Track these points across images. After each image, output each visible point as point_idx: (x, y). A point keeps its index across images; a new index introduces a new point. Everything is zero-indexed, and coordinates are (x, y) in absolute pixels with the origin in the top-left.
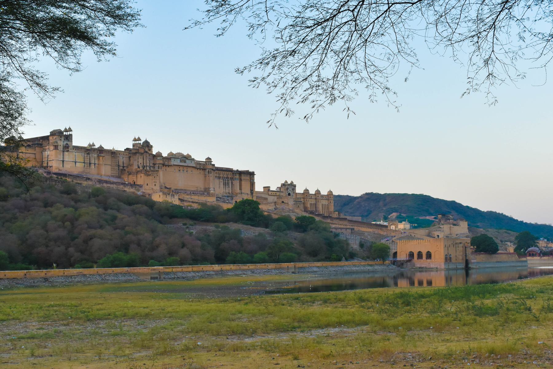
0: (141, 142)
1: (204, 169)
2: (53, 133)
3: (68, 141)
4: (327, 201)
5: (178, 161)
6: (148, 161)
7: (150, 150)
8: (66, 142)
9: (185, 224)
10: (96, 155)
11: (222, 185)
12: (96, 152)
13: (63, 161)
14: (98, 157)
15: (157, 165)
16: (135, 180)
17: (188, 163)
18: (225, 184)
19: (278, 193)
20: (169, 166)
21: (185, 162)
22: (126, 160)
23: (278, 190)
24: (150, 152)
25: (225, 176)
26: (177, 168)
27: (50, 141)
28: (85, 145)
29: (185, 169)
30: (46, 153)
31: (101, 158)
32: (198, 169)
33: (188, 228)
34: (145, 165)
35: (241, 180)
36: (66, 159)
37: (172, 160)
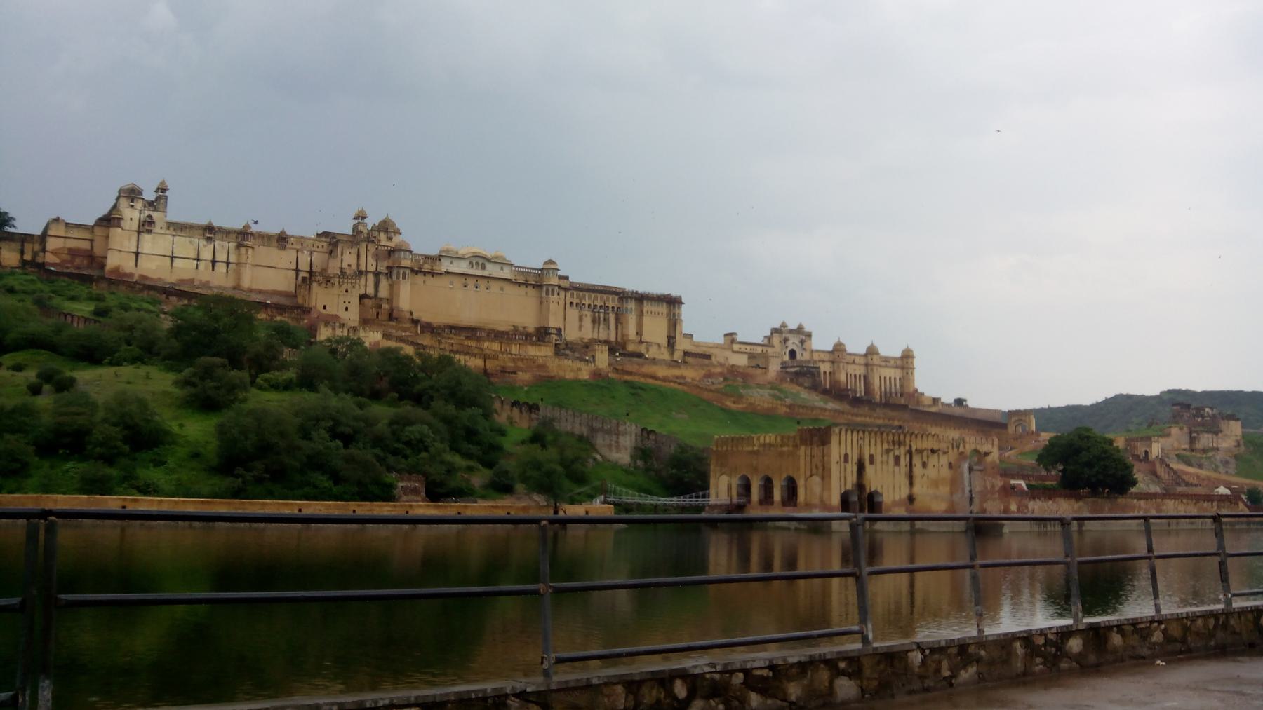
0: (372, 221)
1: (538, 286)
3: (156, 210)
6: (371, 261)
7: (390, 239)
10: (233, 245)
11: (587, 322)
13: (137, 254)
14: (239, 246)
15: (395, 271)
17: (492, 270)
18: (595, 321)
20: (433, 274)
21: (483, 267)
22: (318, 259)
25: (599, 303)
26: (458, 282)
29: (483, 284)
31: (243, 250)
32: (520, 284)
35: (641, 315)
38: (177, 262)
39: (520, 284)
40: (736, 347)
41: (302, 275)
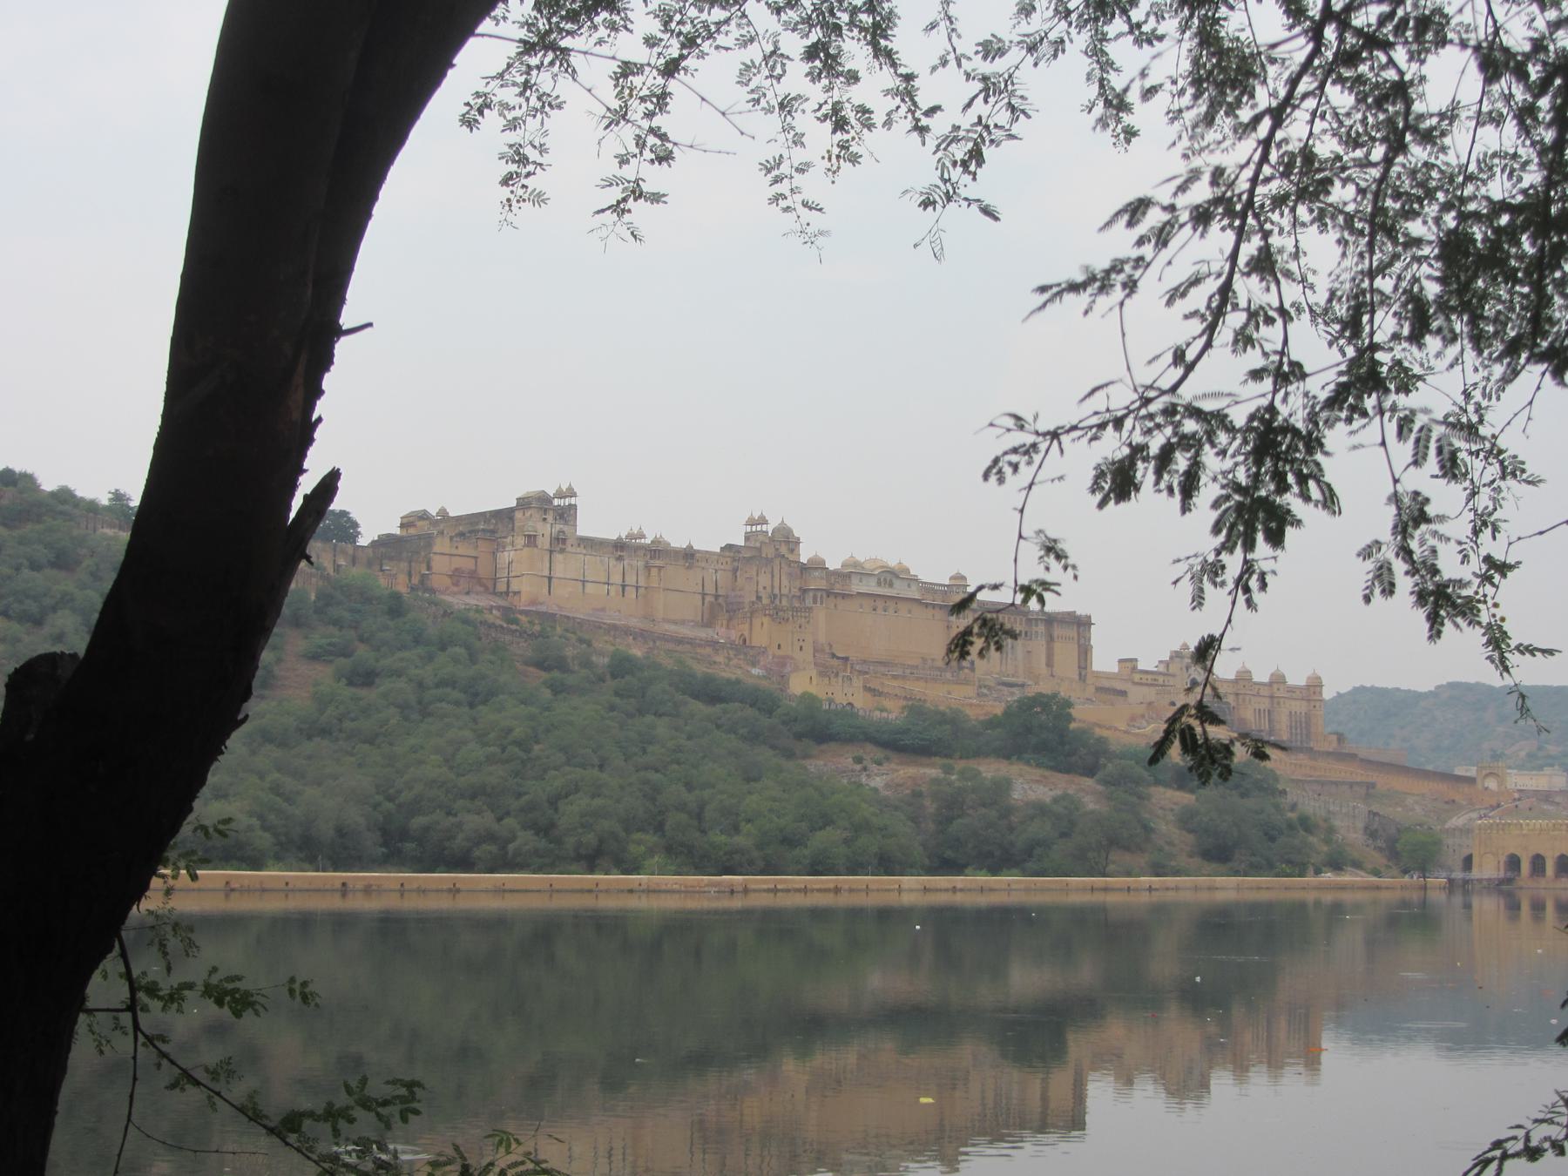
0: (769, 528)
2: (524, 503)
3: (566, 523)
4: (1304, 703)
5: (873, 582)
6: (785, 582)
7: (792, 551)
8: (558, 527)
9: (858, 760)
10: (641, 564)
12: (641, 553)
13: (550, 579)
14: (648, 568)
16: (746, 634)
17: (899, 589)
19: (1161, 679)
20: (844, 596)
21: (891, 585)
23: (1162, 669)
24: (791, 557)
27: (517, 524)
28: (611, 534)
29: (891, 605)
30: (505, 557)
31: (654, 572)
33: (865, 769)
34: (776, 591)
36: (559, 571)
37: (855, 580)
38: (590, 588)
39: (927, 605)
40: (1137, 677)
41: (708, 599)
